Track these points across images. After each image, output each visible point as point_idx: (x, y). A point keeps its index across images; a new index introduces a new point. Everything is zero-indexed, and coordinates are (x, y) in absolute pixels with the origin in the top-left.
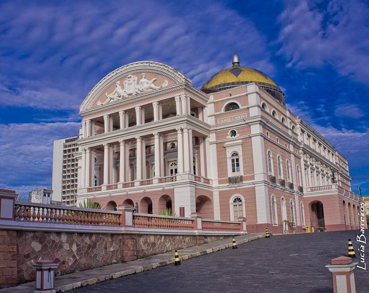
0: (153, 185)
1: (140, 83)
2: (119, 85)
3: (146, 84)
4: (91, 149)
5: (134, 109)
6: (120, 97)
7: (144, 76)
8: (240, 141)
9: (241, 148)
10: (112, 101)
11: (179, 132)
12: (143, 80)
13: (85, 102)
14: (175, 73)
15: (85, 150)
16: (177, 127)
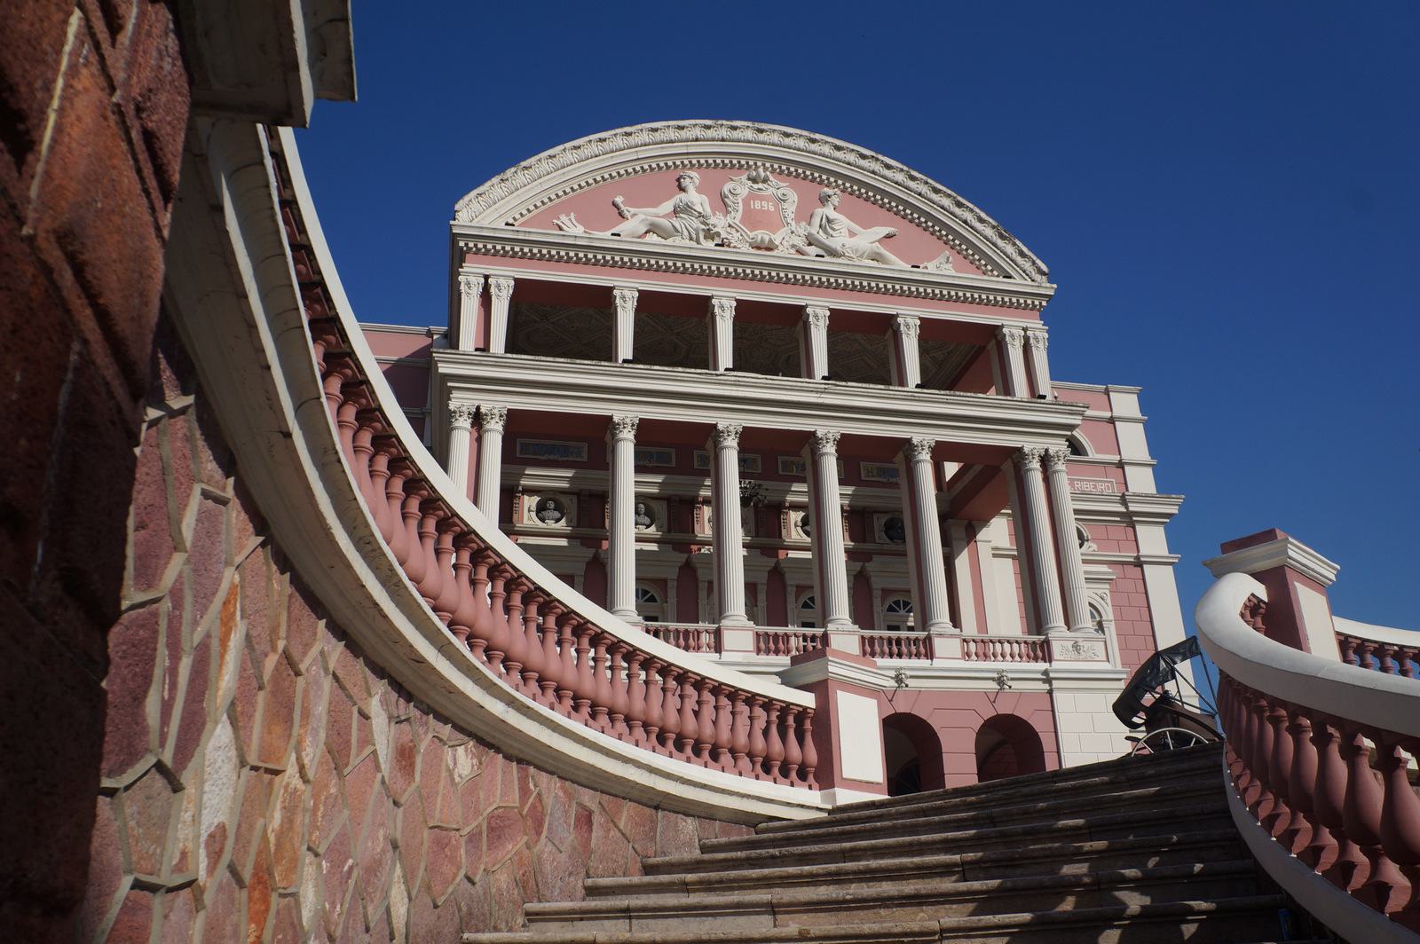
0: (937, 663)
1: (816, 221)
2: (699, 190)
3: (858, 240)
4: (516, 423)
5: (800, 310)
6: (710, 235)
7: (835, 200)
8: (1104, 568)
9: (1107, 592)
10: (652, 238)
11: (1035, 464)
12: (829, 211)
13: (493, 187)
14: (1000, 242)
15: (478, 419)
16: (1032, 445)
